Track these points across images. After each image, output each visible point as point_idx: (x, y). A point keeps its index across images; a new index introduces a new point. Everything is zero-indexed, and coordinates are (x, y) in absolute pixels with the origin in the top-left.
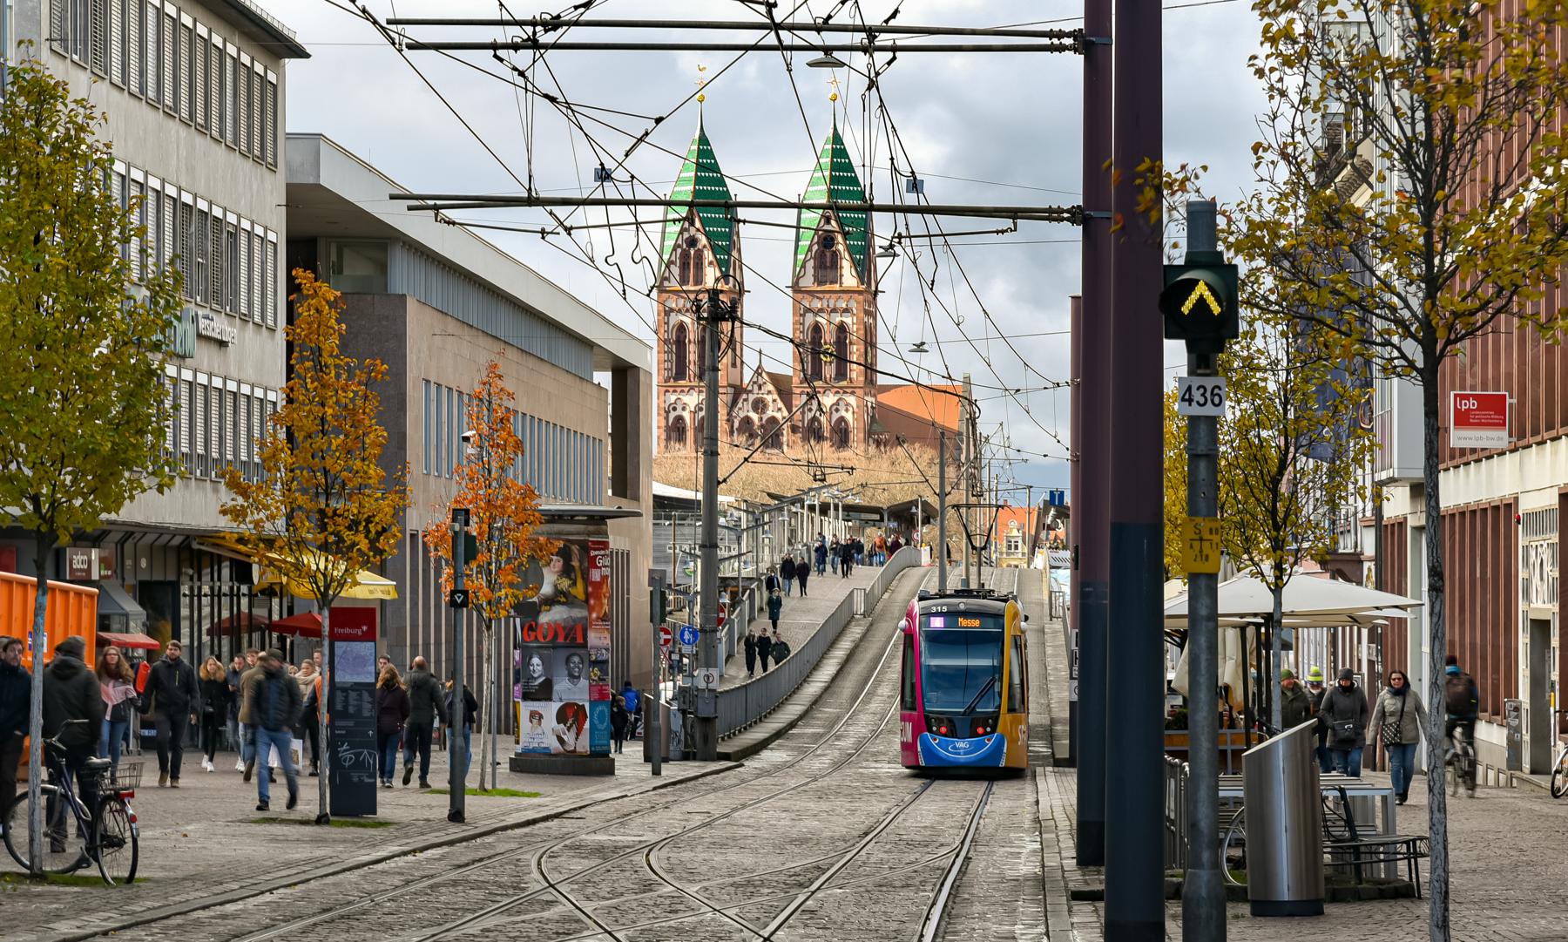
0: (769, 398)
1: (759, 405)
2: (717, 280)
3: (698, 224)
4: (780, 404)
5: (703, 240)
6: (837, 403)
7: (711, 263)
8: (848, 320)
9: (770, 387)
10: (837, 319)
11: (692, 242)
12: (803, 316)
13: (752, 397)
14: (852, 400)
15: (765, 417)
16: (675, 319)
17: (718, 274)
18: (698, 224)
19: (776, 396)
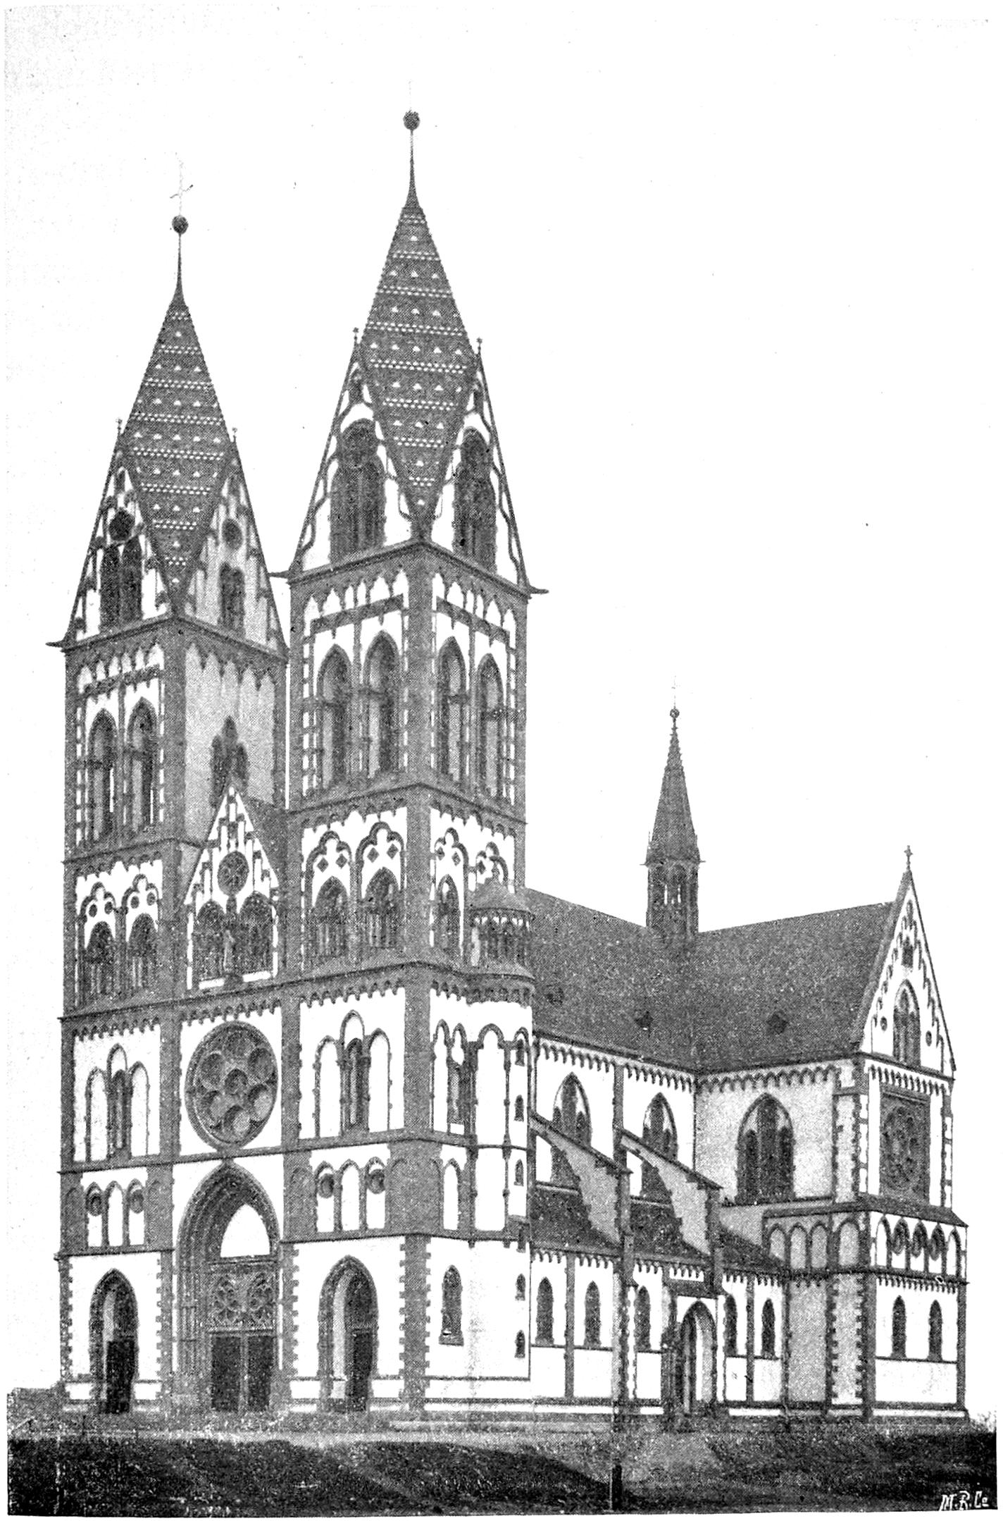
0: (247, 850)
1: (235, 870)
2: (160, 599)
3: (128, 485)
4: (267, 865)
5: (139, 520)
6: (370, 840)
7: (150, 564)
8: (394, 624)
9: (247, 826)
10: (371, 628)
11: (121, 525)
12: (311, 639)
13: (218, 856)
14: (398, 820)
15: (241, 897)
16: (93, 709)
17: (161, 588)
18: (128, 485)
19: (258, 846)
